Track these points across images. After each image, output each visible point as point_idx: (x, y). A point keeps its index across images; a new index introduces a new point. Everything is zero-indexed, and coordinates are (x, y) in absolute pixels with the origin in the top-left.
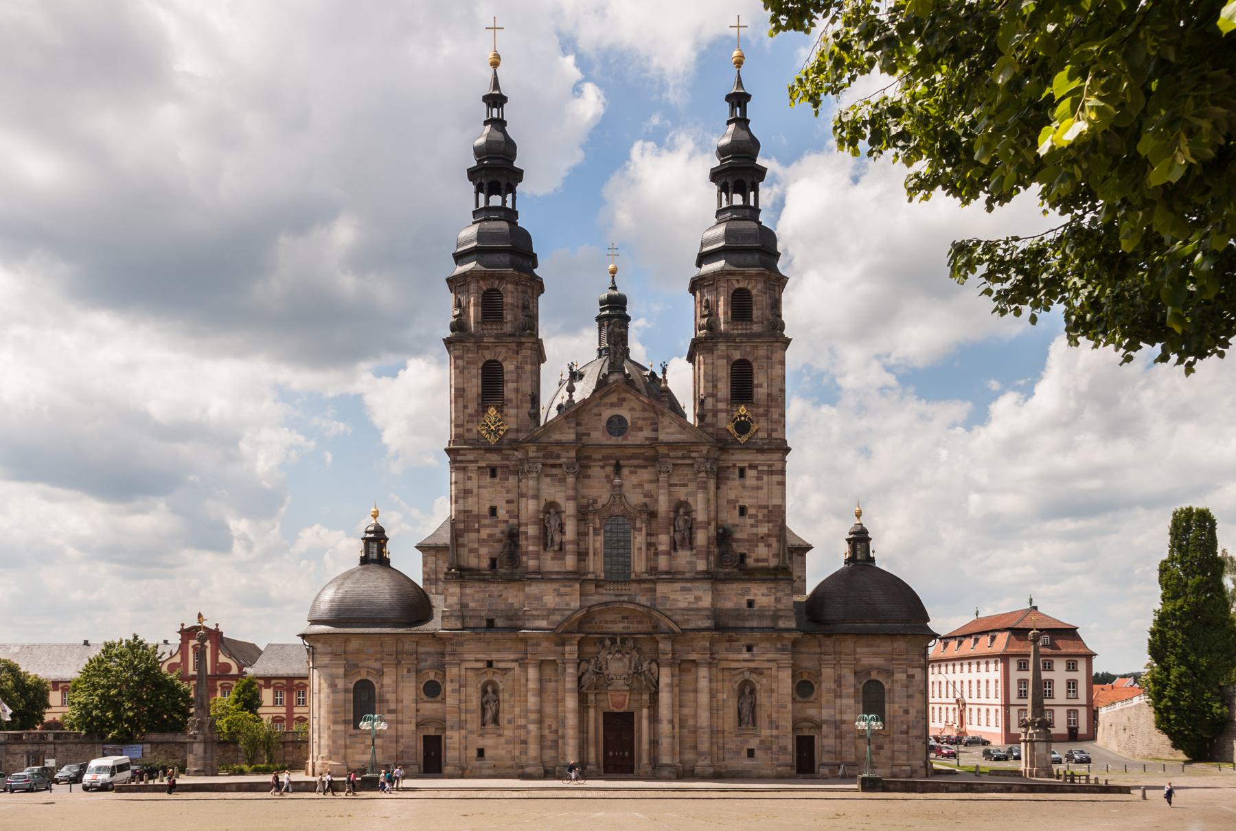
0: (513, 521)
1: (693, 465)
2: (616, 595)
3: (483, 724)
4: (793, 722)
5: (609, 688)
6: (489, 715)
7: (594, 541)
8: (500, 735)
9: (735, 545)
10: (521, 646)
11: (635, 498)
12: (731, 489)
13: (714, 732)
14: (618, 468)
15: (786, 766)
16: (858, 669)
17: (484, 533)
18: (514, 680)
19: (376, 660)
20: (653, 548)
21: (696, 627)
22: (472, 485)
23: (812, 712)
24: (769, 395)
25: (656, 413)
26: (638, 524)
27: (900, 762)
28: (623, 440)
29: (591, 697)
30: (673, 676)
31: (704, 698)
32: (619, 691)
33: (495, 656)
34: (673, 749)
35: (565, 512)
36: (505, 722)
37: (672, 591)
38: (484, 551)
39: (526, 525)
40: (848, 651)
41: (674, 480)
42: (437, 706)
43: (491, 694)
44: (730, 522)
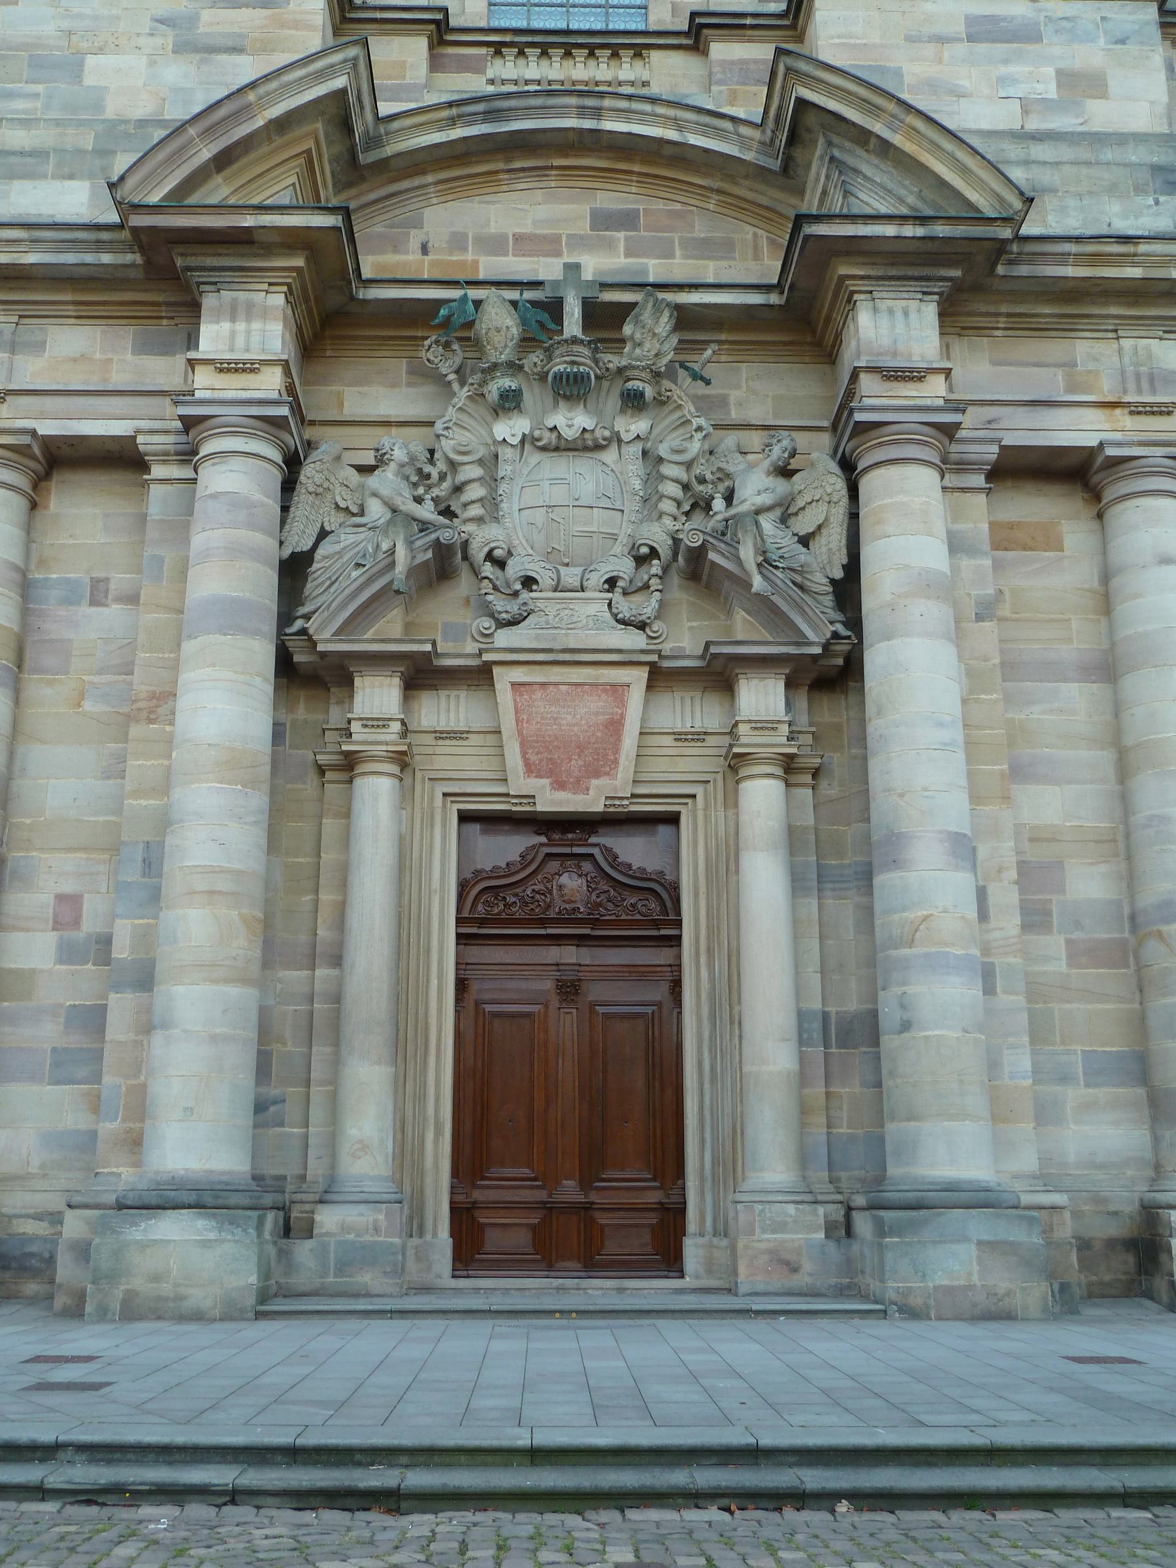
5: (503, 638)
30: (956, 546)
32: (571, 658)
37: (909, 39)
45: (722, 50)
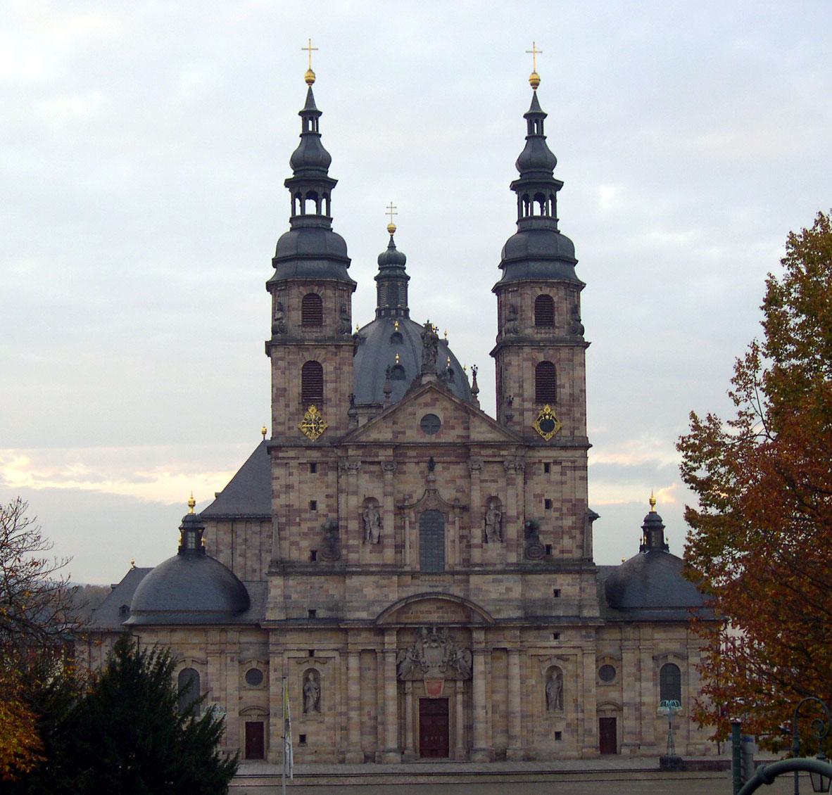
0: (333, 515)
1: (502, 462)
2: (430, 586)
3: (305, 711)
4: (597, 705)
5: (425, 676)
6: (311, 702)
7: (410, 534)
8: (321, 722)
9: (541, 537)
10: (341, 636)
11: (447, 494)
12: (537, 484)
13: (524, 716)
15: (591, 747)
16: (656, 653)
17: (305, 527)
18: (335, 669)
19: (200, 649)
20: (465, 541)
21: (507, 617)
22: (294, 480)
23: (613, 695)
24: (572, 395)
25: (466, 412)
26: (451, 518)
27: (694, 741)
29: (409, 685)
30: (486, 663)
31: (516, 685)
33: (315, 646)
34: (486, 733)
35: (383, 507)
36: (326, 709)
38: (304, 544)
39: (347, 519)
40: (647, 637)
41: (485, 476)
42: (258, 694)
43: (312, 683)
44: (536, 515)
45: (457, 577)
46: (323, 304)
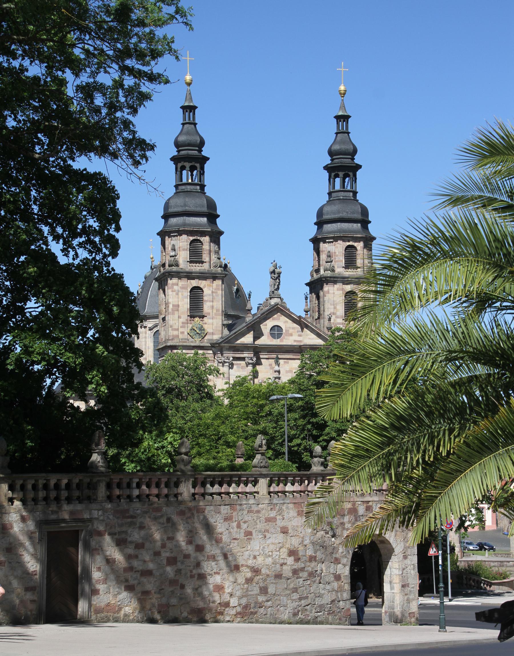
14: (277, 359)
28: (280, 341)
46: (204, 247)
